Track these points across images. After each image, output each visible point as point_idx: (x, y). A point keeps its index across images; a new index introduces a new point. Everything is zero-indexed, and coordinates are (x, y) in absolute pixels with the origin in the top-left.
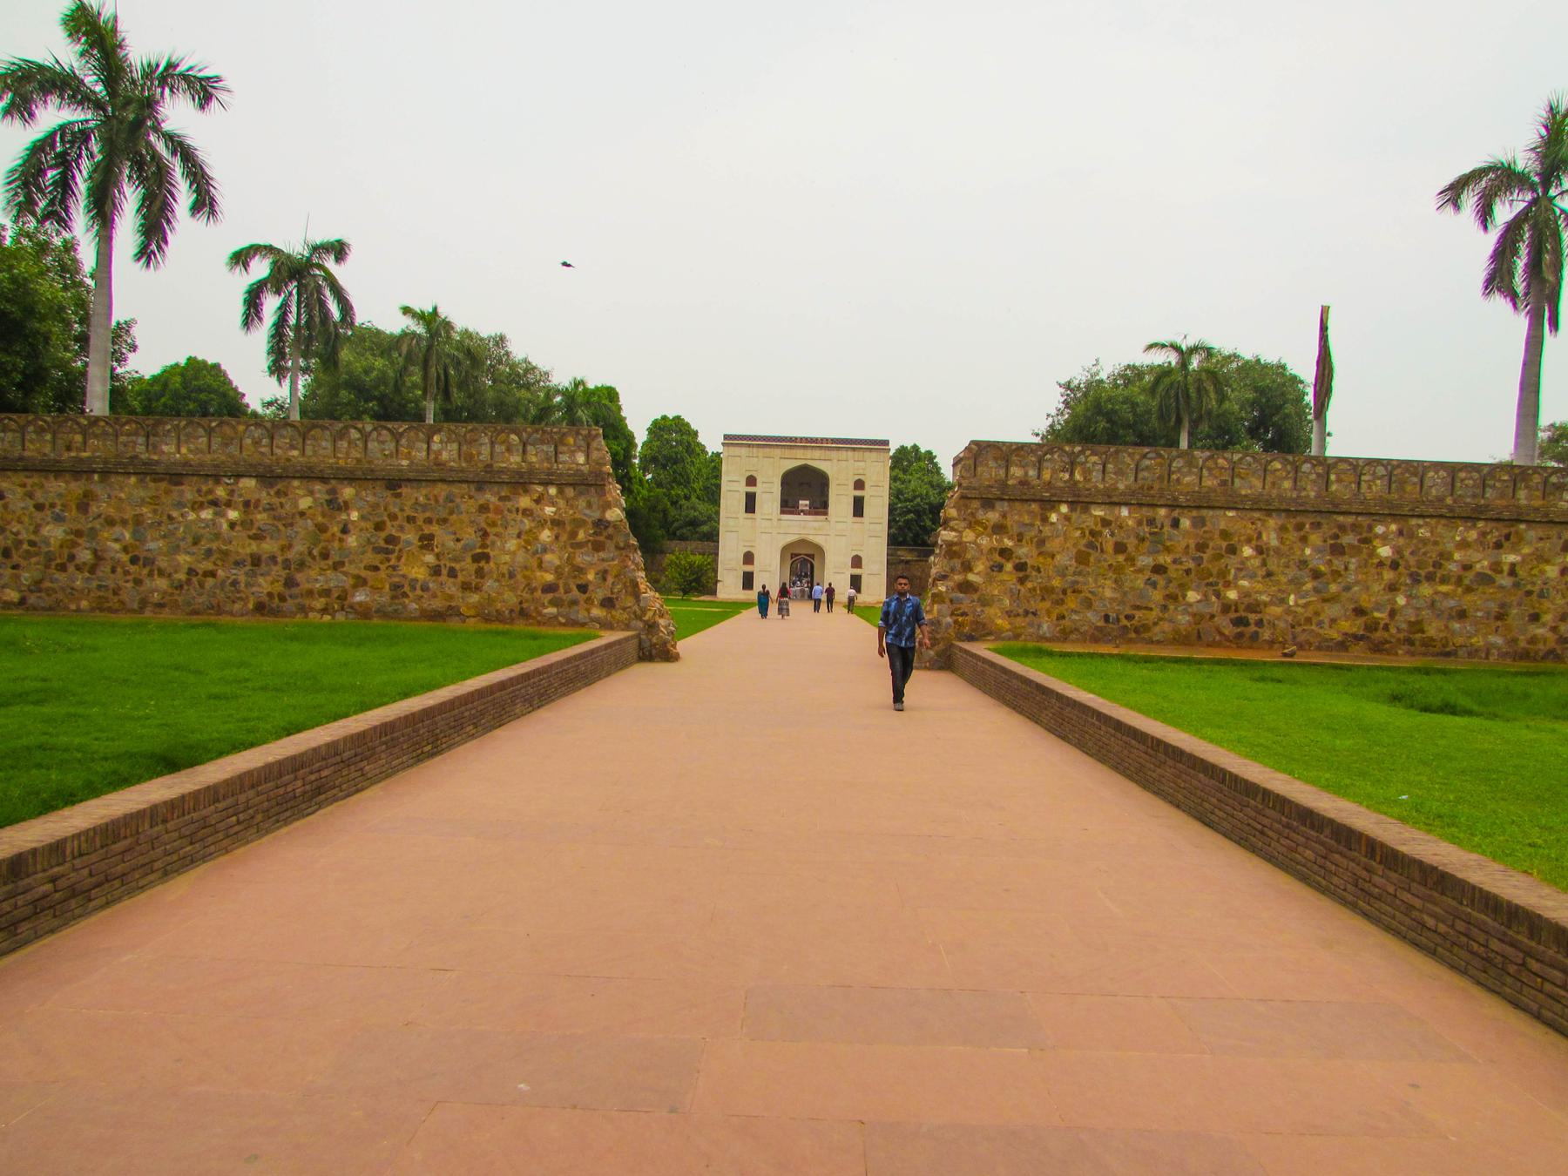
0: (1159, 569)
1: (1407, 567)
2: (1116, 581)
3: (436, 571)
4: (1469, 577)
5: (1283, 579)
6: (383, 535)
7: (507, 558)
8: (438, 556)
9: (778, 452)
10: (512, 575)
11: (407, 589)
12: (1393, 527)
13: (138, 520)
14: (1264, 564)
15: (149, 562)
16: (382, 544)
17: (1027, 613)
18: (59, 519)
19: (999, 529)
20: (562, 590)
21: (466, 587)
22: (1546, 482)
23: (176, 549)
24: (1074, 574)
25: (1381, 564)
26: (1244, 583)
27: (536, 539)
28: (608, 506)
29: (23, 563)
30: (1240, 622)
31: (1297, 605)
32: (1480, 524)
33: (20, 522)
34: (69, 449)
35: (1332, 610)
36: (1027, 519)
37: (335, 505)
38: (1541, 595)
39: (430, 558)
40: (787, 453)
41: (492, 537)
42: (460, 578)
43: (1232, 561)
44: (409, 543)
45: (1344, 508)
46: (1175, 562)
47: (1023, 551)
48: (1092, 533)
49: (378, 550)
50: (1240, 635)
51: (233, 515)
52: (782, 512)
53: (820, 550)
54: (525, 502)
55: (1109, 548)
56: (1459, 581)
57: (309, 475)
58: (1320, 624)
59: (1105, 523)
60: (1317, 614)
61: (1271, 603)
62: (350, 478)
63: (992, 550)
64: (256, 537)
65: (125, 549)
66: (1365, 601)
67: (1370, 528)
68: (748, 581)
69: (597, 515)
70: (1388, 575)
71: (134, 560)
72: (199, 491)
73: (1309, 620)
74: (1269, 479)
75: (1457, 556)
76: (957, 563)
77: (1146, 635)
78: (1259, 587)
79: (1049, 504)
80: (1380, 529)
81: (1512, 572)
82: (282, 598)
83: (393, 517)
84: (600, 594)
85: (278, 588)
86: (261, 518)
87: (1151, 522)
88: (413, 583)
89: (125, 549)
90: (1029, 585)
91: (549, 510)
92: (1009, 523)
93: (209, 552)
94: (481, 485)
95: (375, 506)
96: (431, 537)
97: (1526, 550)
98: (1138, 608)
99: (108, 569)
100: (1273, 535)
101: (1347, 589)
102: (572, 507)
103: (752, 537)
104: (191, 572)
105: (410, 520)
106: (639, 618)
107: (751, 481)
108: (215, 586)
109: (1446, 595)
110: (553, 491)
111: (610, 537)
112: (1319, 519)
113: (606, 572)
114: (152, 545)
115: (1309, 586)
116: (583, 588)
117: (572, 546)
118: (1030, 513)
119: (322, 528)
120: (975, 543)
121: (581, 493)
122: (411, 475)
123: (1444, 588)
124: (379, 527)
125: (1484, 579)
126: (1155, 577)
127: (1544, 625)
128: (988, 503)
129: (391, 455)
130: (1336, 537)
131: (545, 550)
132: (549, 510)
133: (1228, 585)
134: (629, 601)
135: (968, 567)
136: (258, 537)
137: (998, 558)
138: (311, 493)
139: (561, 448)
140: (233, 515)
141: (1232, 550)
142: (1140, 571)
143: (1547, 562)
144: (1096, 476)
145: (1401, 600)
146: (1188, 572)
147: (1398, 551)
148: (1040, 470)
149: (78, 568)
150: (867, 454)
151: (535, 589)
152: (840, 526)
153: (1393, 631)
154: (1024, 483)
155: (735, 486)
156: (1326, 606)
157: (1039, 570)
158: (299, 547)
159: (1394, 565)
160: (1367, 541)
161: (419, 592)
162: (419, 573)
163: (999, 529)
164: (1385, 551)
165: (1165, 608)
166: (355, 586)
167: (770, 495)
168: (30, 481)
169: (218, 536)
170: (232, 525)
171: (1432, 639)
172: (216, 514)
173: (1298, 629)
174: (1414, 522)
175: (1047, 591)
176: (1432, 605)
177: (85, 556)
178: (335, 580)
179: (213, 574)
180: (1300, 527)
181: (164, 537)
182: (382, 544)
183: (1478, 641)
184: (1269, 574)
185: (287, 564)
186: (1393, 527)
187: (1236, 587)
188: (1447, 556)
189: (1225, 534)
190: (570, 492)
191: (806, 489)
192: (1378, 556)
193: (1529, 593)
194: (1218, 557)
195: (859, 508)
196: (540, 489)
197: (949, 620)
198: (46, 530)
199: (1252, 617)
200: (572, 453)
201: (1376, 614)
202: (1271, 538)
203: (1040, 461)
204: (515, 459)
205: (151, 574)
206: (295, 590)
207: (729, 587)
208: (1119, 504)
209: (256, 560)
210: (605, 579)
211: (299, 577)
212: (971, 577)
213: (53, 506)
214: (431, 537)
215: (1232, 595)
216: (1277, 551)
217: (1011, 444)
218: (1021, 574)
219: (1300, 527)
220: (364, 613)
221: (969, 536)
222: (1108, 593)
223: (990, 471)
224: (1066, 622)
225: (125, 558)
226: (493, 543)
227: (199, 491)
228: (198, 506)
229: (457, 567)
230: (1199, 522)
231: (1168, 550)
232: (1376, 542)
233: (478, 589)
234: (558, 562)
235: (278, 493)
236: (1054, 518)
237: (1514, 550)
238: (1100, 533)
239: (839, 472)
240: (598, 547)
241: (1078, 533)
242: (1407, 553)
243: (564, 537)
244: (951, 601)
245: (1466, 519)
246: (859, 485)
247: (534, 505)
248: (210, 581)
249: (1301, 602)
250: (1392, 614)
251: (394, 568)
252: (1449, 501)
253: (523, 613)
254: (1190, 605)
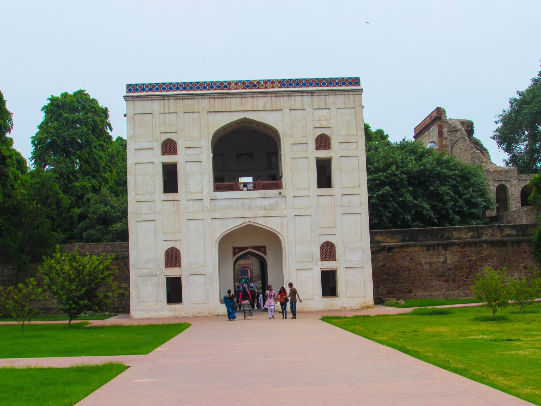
9: (205, 103)
40: (218, 104)
52: (217, 189)
53: (274, 239)
68: (174, 291)
103: (176, 225)
107: (169, 147)
150: (330, 99)
152: (301, 202)
155: (145, 156)
167: (197, 167)
191: (247, 154)
195: (324, 176)
207: (147, 301)
239: (293, 126)
246: (323, 142)
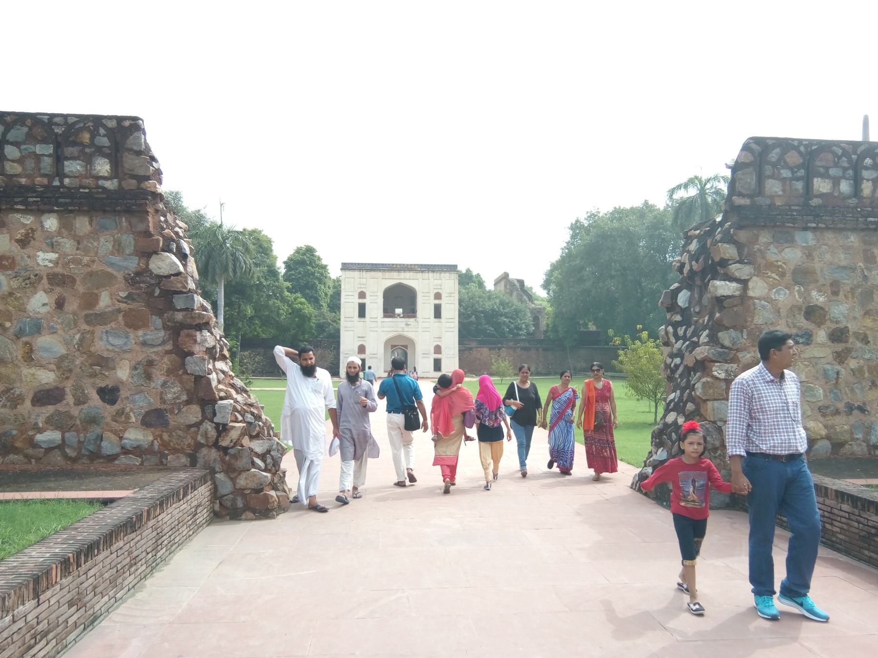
17: (850, 408)
19: (802, 276)
20: (70, 399)
27: (22, 309)
36: (842, 259)
47: (840, 310)
63: (794, 309)
84: (138, 403)
90: (853, 364)
91: (45, 258)
92: (817, 265)
102: (86, 251)
110: (51, 223)
113: (150, 363)
116: (109, 394)
117: (88, 320)
118: (846, 249)
121: (104, 228)
131: (37, 328)
132: (45, 258)
139: (69, 151)
148: (857, 182)
151: (20, 399)
152: (427, 325)
157: (865, 340)
163: (802, 276)
190: (82, 224)
195: (438, 313)
196: (28, 220)
200: (89, 160)
210: (149, 377)
217: (811, 142)
218: (839, 347)
234: (62, 350)
240: (134, 322)
243: (72, 305)
246: (438, 296)
247: (15, 249)
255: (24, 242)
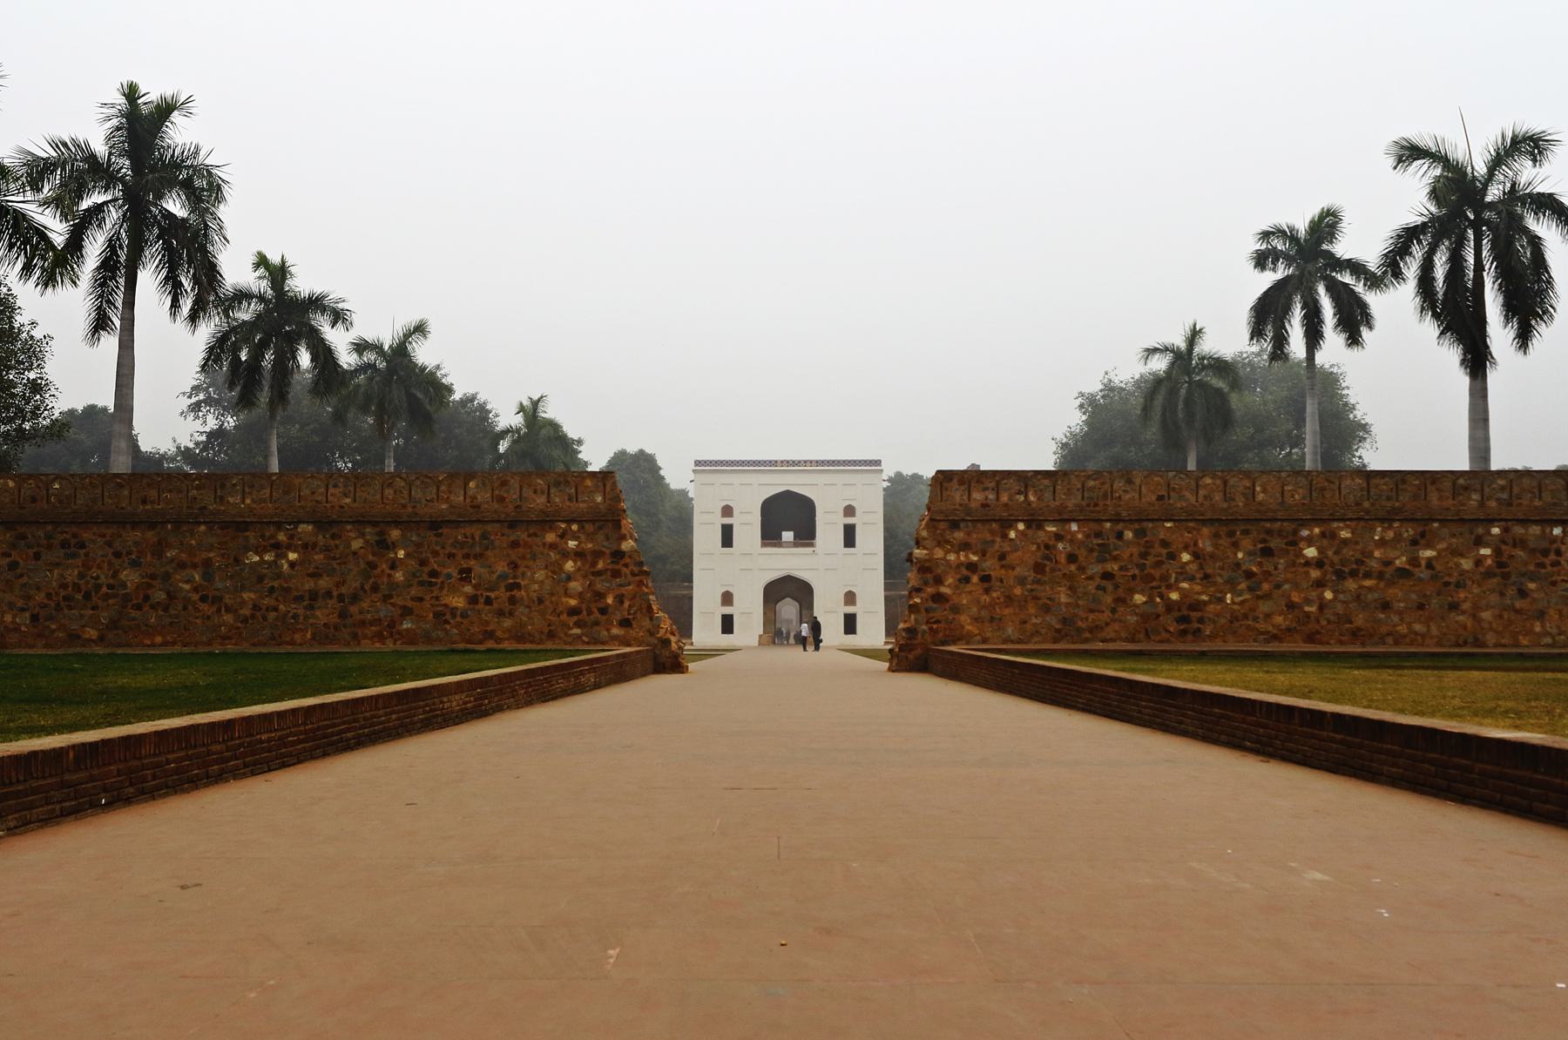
0: (1107, 576)
1: (1332, 564)
2: (1070, 588)
3: (473, 600)
4: (1389, 570)
5: (1220, 580)
6: (427, 569)
7: (536, 587)
8: (475, 587)
10: (540, 601)
11: (448, 617)
12: (1317, 530)
13: (207, 563)
14: (1201, 567)
15: (217, 600)
16: (425, 577)
18: (135, 564)
21: (500, 613)
22: (1454, 484)
23: (243, 588)
24: (1034, 582)
25: (1308, 563)
26: (1185, 585)
27: (561, 569)
28: (623, 538)
29: (100, 603)
30: (1184, 619)
31: (1233, 602)
32: (1396, 525)
33: (99, 567)
34: (144, 502)
35: (1264, 607)
36: (989, 537)
37: (384, 545)
38: (1458, 585)
39: (468, 589)
41: (521, 570)
42: (496, 605)
43: (1171, 569)
44: (449, 576)
45: (1270, 515)
46: (1121, 568)
47: (990, 566)
48: (1047, 547)
49: (421, 583)
50: (1184, 633)
51: (292, 556)
54: (551, 537)
55: (1063, 559)
56: (1381, 576)
57: (360, 522)
58: (1256, 619)
59: (1058, 537)
60: (1253, 610)
61: (1210, 602)
62: (397, 523)
64: (311, 575)
65: (196, 590)
66: (1296, 598)
67: (1295, 532)
69: (615, 547)
70: (1315, 574)
71: (203, 599)
72: (262, 536)
73: (1246, 616)
74: (1202, 492)
75: (1377, 554)
76: (929, 576)
77: (1100, 635)
78: (1198, 588)
79: (1008, 523)
80: (1305, 533)
81: (1430, 564)
82: (336, 628)
83: (436, 554)
85: (334, 619)
86: (319, 557)
87: (1098, 535)
88: (454, 611)
89: (196, 590)
91: (572, 544)
93: (272, 589)
94: (513, 525)
95: (419, 545)
96: (469, 570)
97: (1441, 546)
98: (1092, 611)
99: (180, 607)
100: (1208, 543)
101: (1278, 586)
104: (256, 607)
105: (451, 556)
106: (652, 634)
108: (276, 619)
109: (1370, 589)
110: (575, 527)
111: (626, 565)
112: (1248, 527)
114: (220, 585)
115: (1243, 586)
118: (992, 532)
119: (372, 566)
120: (944, 559)
121: (600, 528)
122: (453, 518)
123: (1368, 583)
124: (423, 563)
125: (1403, 573)
126: (1104, 583)
127: (1464, 612)
128: (955, 525)
129: (431, 501)
130: (1264, 541)
131: (569, 578)
133: (1170, 587)
134: (647, 623)
135: (939, 581)
136: (315, 575)
137: (965, 572)
138: (363, 535)
140: (292, 556)
141: (1173, 556)
142: (1091, 578)
143: (1462, 555)
144: (1048, 495)
145: (1328, 595)
146: (1134, 577)
147: (1321, 550)
149: (152, 607)
153: (1324, 623)
154: (984, 505)
156: (1261, 603)
158: (353, 583)
159: (1319, 563)
160: (1294, 543)
161: (458, 619)
162: (458, 602)
163: (965, 546)
164: (1311, 552)
165: (1114, 611)
166: (402, 616)
168: (109, 532)
169: (279, 576)
170: (292, 565)
171: (1359, 629)
172: (278, 556)
173: (1237, 624)
174: (1335, 525)
175: (1009, 599)
176: (1358, 597)
177: (160, 596)
178: (384, 611)
179: (276, 609)
180: (1231, 534)
181: (231, 577)
182: (425, 577)
183: (1402, 629)
184: (1206, 576)
185: (341, 598)
186: (1317, 530)
187: (1178, 589)
188: (1370, 555)
189: (1164, 544)
190: (589, 527)
192: (1304, 556)
193: (1447, 584)
194: (1159, 564)
197: (925, 627)
198: (123, 575)
199: (1194, 615)
201: (1307, 609)
202: (1206, 545)
203: (998, 483)
204: (541, 500)
205: (219, 610)
206: (349, 621)
208: (1069, 521)
209: (314, 595)
210: (622, 602)
211: (353, 609)
212: (943, 590)
213: (129, 553)
214: (469, 570)
215: (1174, 596)
216: (1212, 556)
219: (1231, 534)
220: (410, 638)
221: (939, 553)
222: (1063, 599)
223: (957, 494)
224: (1028, 626)
225: (195, 597)
226: (523, 574)
227: (262, 536)
228: (259, 551)
229: (492, 595)
230: (1140, 533)
231: (1115, 559)
232: (1302, 545)
233: (511, 614)
235: (333, 537)
236: (1012, 535)
237: (1429, 546)
238: (1055, 547)
240: (616, 574)
241: (1034, 548)
242: (1330, 553)
244: (927, 610)
245: (1382, 520)
248: (272, 615)
249: (1238, 599)
250: (1321, 608)
251: (437, 598)
252: (1366, 504)
253: (551, 635)
254: (1137, 606)
255: (562, 536)
